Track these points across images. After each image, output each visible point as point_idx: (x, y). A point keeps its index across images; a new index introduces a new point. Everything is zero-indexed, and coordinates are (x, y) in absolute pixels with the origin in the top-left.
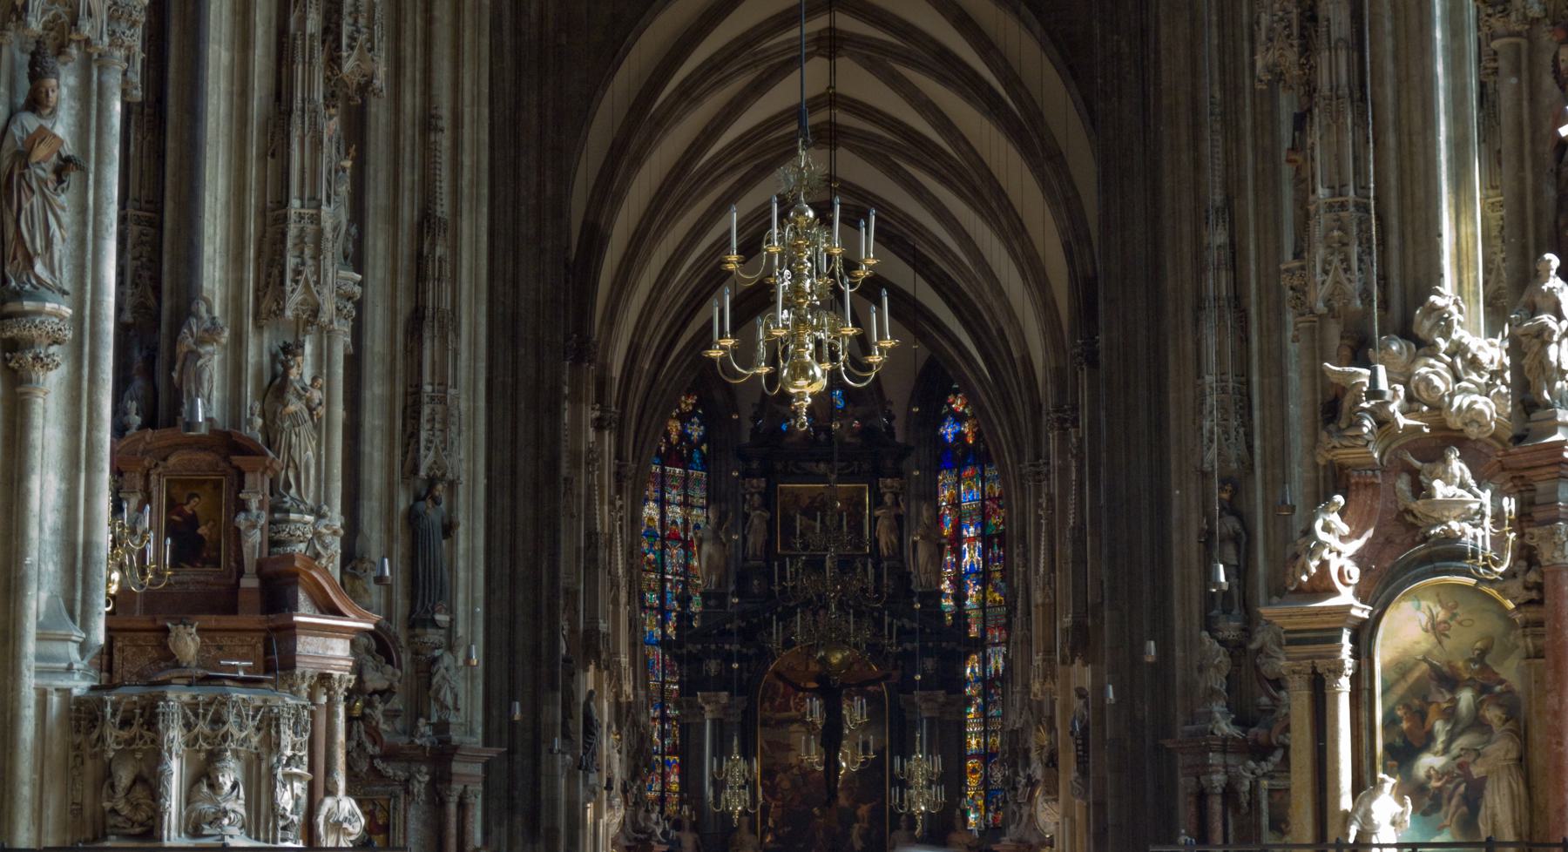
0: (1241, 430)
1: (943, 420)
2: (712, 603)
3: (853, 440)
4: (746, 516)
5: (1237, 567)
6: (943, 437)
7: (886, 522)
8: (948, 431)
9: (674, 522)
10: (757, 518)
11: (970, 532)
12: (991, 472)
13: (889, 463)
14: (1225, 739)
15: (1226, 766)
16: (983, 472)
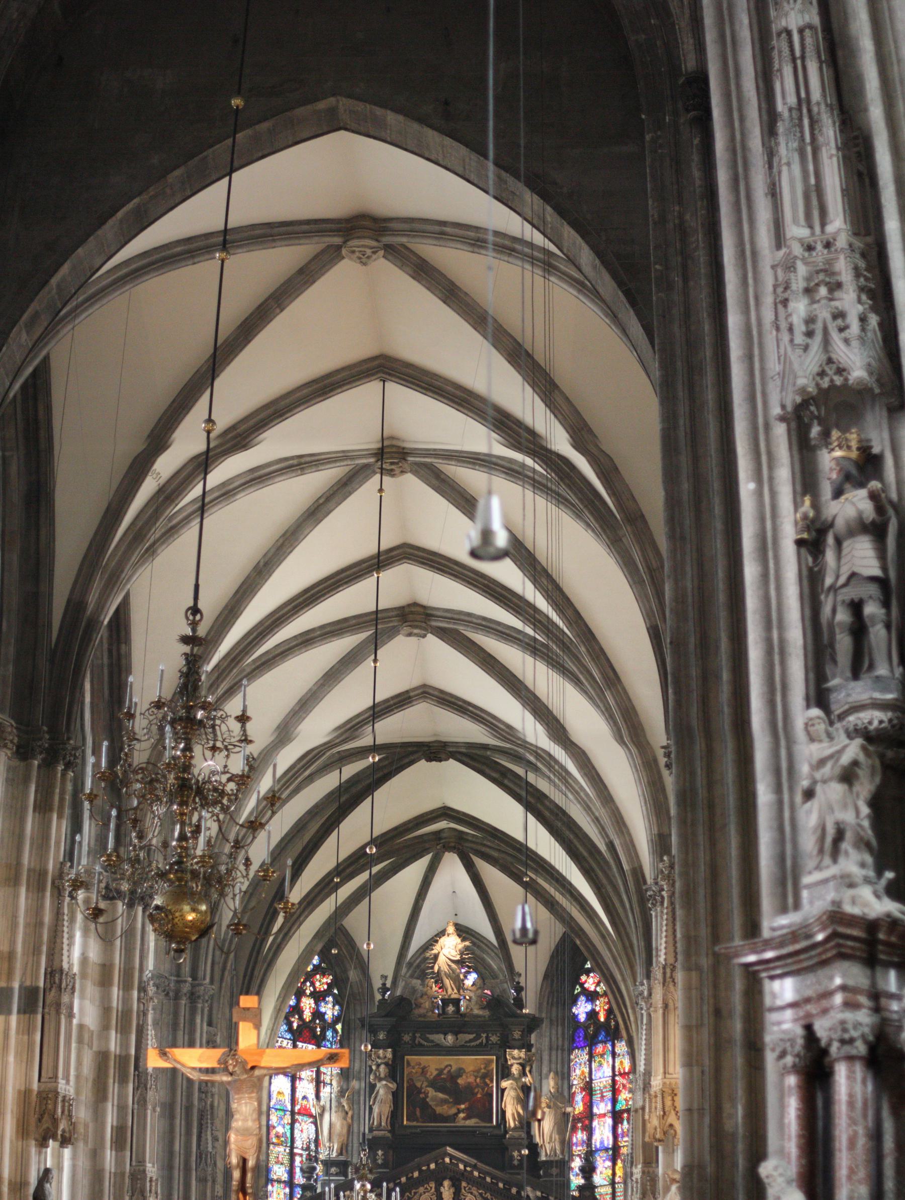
0: (874, 320)
1: (574, 1001)
2: (333, 1170)
3: (481, 1012)
4: (372, 1087)
5: (882, 582)
6: (575, 1017)
7: (513, 1093)
8: (582, 1009)
9: (305, 1098)
10: (383, 1090)
11: (602, 1107)
12: (621, 1047)
13: (517, 1035)
14: (872, 926)
15: (877, 996)
16: (613, 1046)
